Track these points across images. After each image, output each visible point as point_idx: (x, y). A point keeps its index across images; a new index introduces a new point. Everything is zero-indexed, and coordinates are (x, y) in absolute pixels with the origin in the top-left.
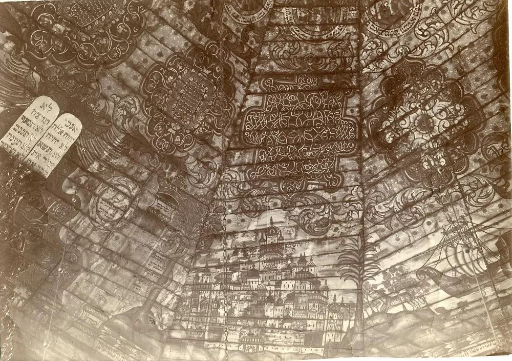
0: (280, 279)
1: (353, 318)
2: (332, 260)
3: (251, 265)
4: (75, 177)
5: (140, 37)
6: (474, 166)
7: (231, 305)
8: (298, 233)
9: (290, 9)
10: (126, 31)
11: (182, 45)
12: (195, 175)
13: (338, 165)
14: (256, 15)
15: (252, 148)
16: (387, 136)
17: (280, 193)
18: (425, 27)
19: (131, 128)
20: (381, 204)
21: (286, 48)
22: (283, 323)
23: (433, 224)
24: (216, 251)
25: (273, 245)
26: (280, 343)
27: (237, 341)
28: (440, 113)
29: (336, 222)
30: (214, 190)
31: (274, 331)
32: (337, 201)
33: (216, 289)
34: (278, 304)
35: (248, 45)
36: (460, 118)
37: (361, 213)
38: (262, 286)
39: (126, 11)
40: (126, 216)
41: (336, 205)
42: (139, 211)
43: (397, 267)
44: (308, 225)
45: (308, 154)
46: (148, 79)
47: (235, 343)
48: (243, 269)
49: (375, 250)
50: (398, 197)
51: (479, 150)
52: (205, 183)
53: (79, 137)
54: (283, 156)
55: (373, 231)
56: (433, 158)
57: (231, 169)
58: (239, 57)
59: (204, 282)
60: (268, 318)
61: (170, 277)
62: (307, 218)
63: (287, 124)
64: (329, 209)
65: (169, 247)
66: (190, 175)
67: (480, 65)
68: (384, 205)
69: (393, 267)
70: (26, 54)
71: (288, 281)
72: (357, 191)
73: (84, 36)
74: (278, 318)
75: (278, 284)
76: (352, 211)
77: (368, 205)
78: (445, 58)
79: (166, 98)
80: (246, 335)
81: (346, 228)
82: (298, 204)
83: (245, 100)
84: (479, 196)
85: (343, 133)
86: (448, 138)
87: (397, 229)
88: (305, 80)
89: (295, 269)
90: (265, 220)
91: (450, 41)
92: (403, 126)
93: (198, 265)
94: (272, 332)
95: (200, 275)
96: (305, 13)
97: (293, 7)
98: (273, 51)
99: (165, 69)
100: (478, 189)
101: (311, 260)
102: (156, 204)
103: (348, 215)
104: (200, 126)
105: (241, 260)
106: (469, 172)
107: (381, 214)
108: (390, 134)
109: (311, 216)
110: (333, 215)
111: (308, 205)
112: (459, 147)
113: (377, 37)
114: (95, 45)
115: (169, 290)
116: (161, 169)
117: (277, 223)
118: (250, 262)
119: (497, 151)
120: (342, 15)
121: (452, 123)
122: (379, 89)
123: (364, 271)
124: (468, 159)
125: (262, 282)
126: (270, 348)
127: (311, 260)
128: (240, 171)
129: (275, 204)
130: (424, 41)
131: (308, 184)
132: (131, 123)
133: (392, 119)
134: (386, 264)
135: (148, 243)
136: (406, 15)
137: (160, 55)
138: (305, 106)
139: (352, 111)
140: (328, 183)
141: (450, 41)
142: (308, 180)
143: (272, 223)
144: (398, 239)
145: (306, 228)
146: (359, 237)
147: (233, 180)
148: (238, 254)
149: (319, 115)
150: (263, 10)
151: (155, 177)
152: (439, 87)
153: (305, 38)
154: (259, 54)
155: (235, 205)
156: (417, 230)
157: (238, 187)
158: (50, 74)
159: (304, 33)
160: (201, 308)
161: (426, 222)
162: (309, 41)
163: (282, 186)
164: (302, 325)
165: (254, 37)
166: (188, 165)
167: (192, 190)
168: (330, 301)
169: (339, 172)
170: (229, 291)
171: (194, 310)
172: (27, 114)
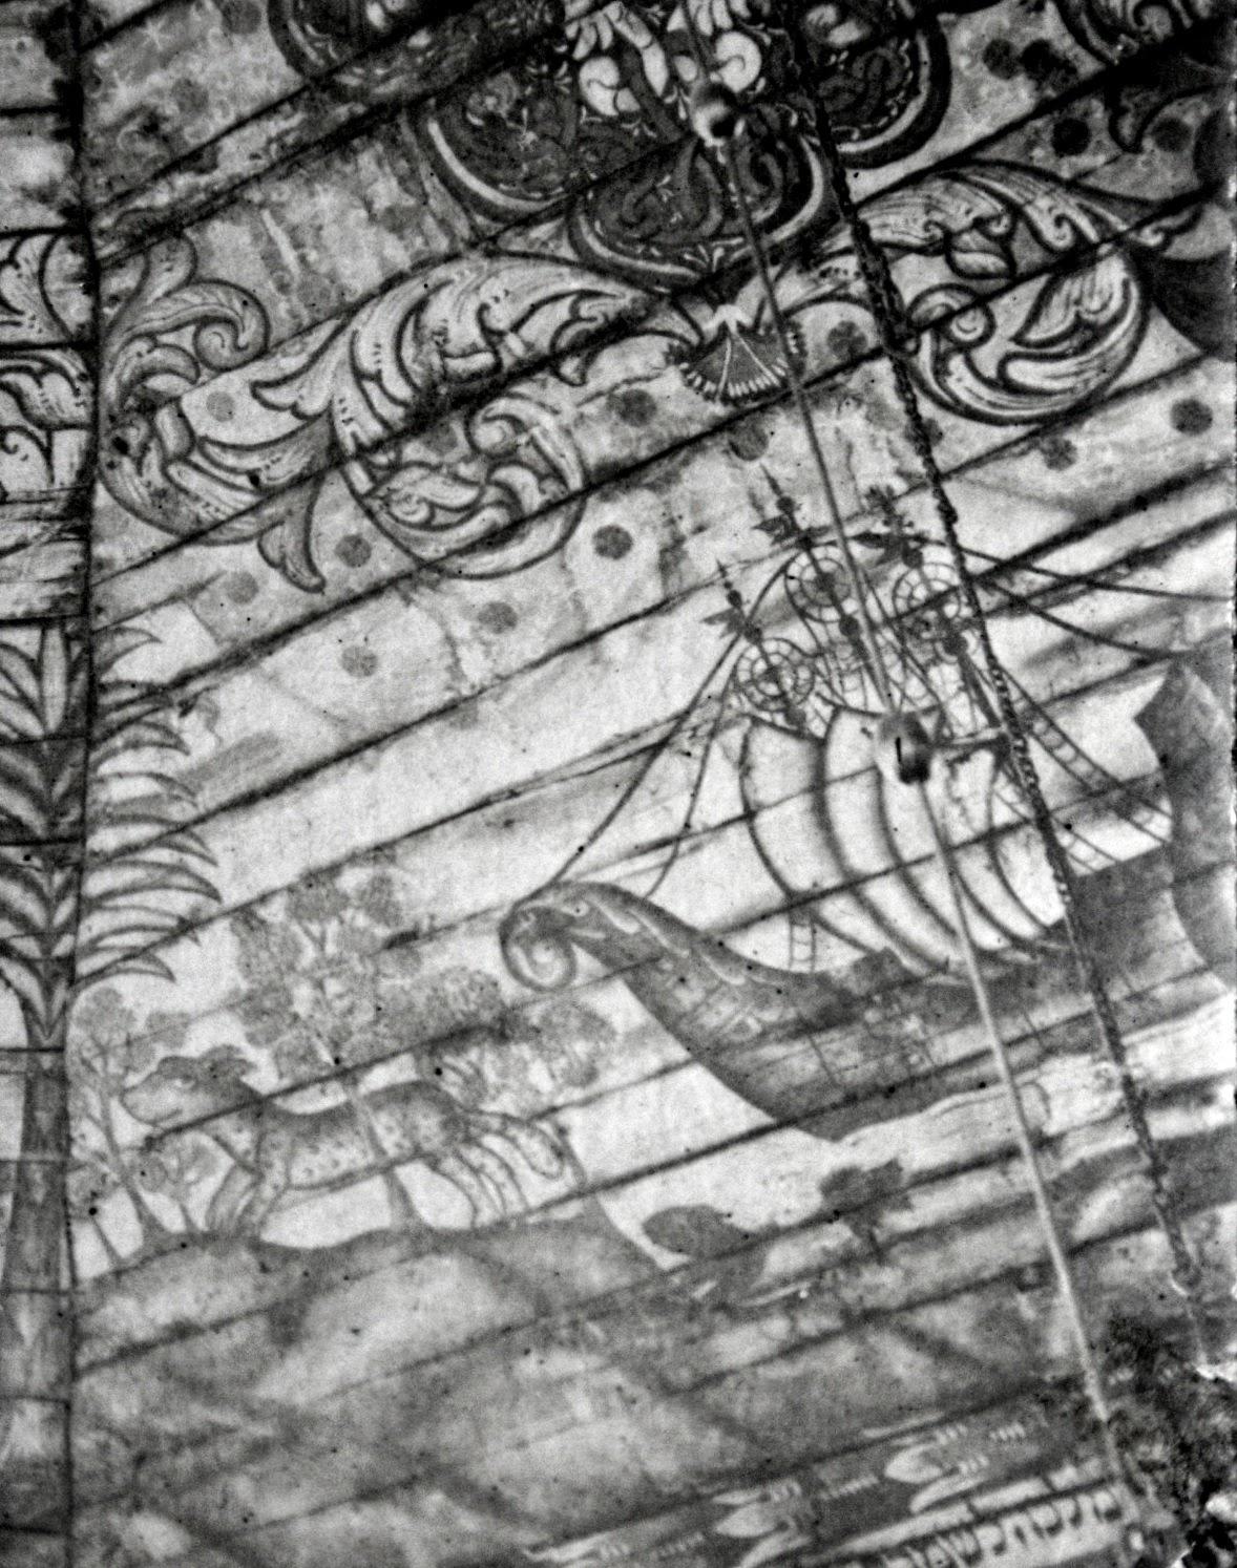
20: (234, 384)
23: (646, 548)
37: (69, 447)
43: (353, 880)
50: (375, 328)
55: (159, 595)
56: (659, 33)
68: (256, 388)
69: (320, 876)
72: (41, 275)
77: (126, 390)
84: (1018, 339)
87: (356, 581)
100: (1014, 278)
106: (948, 141)
107: (230, 460)
123: (86, 906)
144: (361, 663)
146: (55, 638)
156: (515, 591)
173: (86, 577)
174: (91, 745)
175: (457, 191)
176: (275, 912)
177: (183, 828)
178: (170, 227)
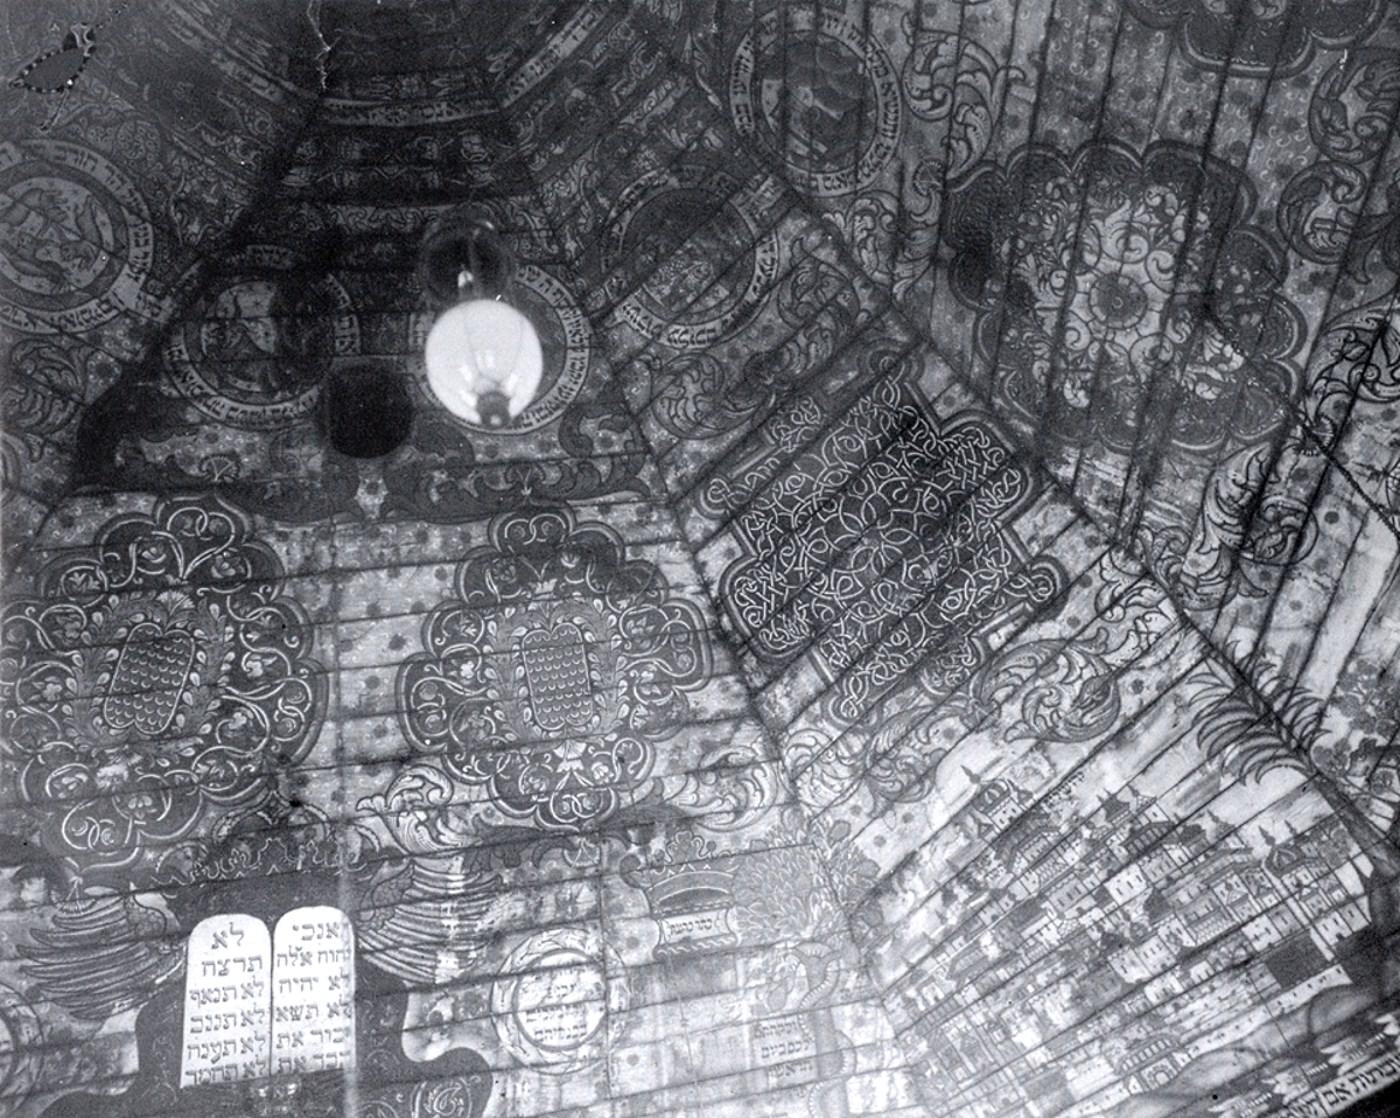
0: (1097, 883)
1: (1355, 849)
2: (1188, 755)
3: (1006, 899)
4: (421, 1018)
5: (317, 647)
6: (1313, 307)
7: (1032, 1011)
8: (1054, 758)
10: (270, 661)
11: (434, 584)
12: (715, 806)
13: (1020, 545)
15: (800, 655)
16: (1068, 394)
17: (939, 703)
18: (924, 82)
19: (465, 833)
20: (1191, 554)
22: (1187, 975)
23: (1344, 513)
24: (904, 922)
25: (1017, 823)
26: (1218, 1020)
27: (1113, 1078)
28: (1127, 247)
29: (1122, 671)
30: (794, 801)
31: (1181, 1002)
32: (1083, 623)
33: (970, 1001)
34: (1139, 941)
35: (600, 456)
36: (1180, 220)
37: (1166, 606)
38: (1069, 927)
39: (236, 624)
40: (614, 1005)
41: (1090, 632)
42: (639, 974)
43: (1352, 667)
44: (1061, 725)
45: (931, 573)
46: (411, 712)
47: (1112, 1084)
48: (994, 918)
49: (1269, 666)
50: (1211, 509)
51: (1292, 256)
52: (756, 801)
53: (357, 936)
54: (877, 618)
55: (1228, 627)
56: (1205, 364)
57: (791, 732)
58: (602, 494)
59: (933, 1003)
60: (1141, 985)
61: (843, 1043)
62: (1046, 712)
63: (830, 546)
64: (1081, 653)
65: (782, 990)
66: (701, 817)
67: (1113, 53)
68: (1197, 551)
69: (1343, 672)
70: (84, 877)
71: (1119, 876)
72: (1115, 567)
73: (182, 745)
74: (1166, 970)
75: (1102, 896)
76: (1142, 618)
77: (1167, 579)
78: (1023, 112)
79: (491, 714)
80: (1124, 1052)
81: (1158, 665)
82: (1000, 695)
83: (700, 567)
84: (1389, 365)
85: (970, 466)
86: (1195, 287)
87: (1274, 585)
88: (789, 422)
89: (1114, 838)
90: (954, 786)
91: (1001, 61)
92: (1080, 346)
93: (890, 977)
94: (1177, 1007)
95: (911, 993)
96: (667, 282)
97: (631, 292)
98: (672, 418)
99: (436, 662)
100: (1370, 349)
101: (1135, 793)
102: (667, 931)
103: (1138, 633)
104: (633, 704)
105: (972, 904)
106: (1313, 327)
107: (1210, 576)
108: (1068, 385)
109: (1053, 700)
110: (1102, 660)
111: (1024, 682)
112: (1240, 289)
113: (856, 195)
114: (226, 741)
115: (869, 1072)
116: (613, 856)
117: (986, 770)
118: (996, 896)
119: (1336, 221)
120: (746, 217)
121: (1176, 246)
122: (961, 308)
123: (1290, 728)
124: (1282, 299)
125: (1061, 916)
126: (1205, 1045)
127: (1135, 793)
128: (814, 722)
129: (949, 734)
130: (952, 116)
131: (984, 639)
132: (454, 823)
133: (1043, 350)
134: (1321, 678)
135: (718, 1018)
136: (864, 93)
137: (397, 643)
138: (835, 478)
139: (950, 402)
140: (1028, 599)
141: (1001, 61)
142: (976, 629)
143: (975, 778)
144: (1296, 606)
145: (1064, 733)
146: (1210, 661)
147: (815, 750)
148: (956, 897)
149: (882, 470)
150: (571, 354)
151: (614, 881)
152: (1072, 190)
153: (711, 335)
154: (649, 450)
155: (863, 798)
156: (1319, 552)
157: (839, 759)
158: (179, 873)
159: (701, 327)
160: (974, 1061)
161: (1321, 520)
162: (725, 333)
163: (930, 682)
164: (1237, 948)
166: (676, 802)
167: (736, 840)
168: (1261, 850)
169: (1040, 557)
170: (1003, 984)
171: (959, 1073)
172: (195, 981)
173: (1205, 637)
174: (1249, 683)
175: (1194, 453)
176: (1340, 693)
177: (1294, 687)
178: (1137, 526)
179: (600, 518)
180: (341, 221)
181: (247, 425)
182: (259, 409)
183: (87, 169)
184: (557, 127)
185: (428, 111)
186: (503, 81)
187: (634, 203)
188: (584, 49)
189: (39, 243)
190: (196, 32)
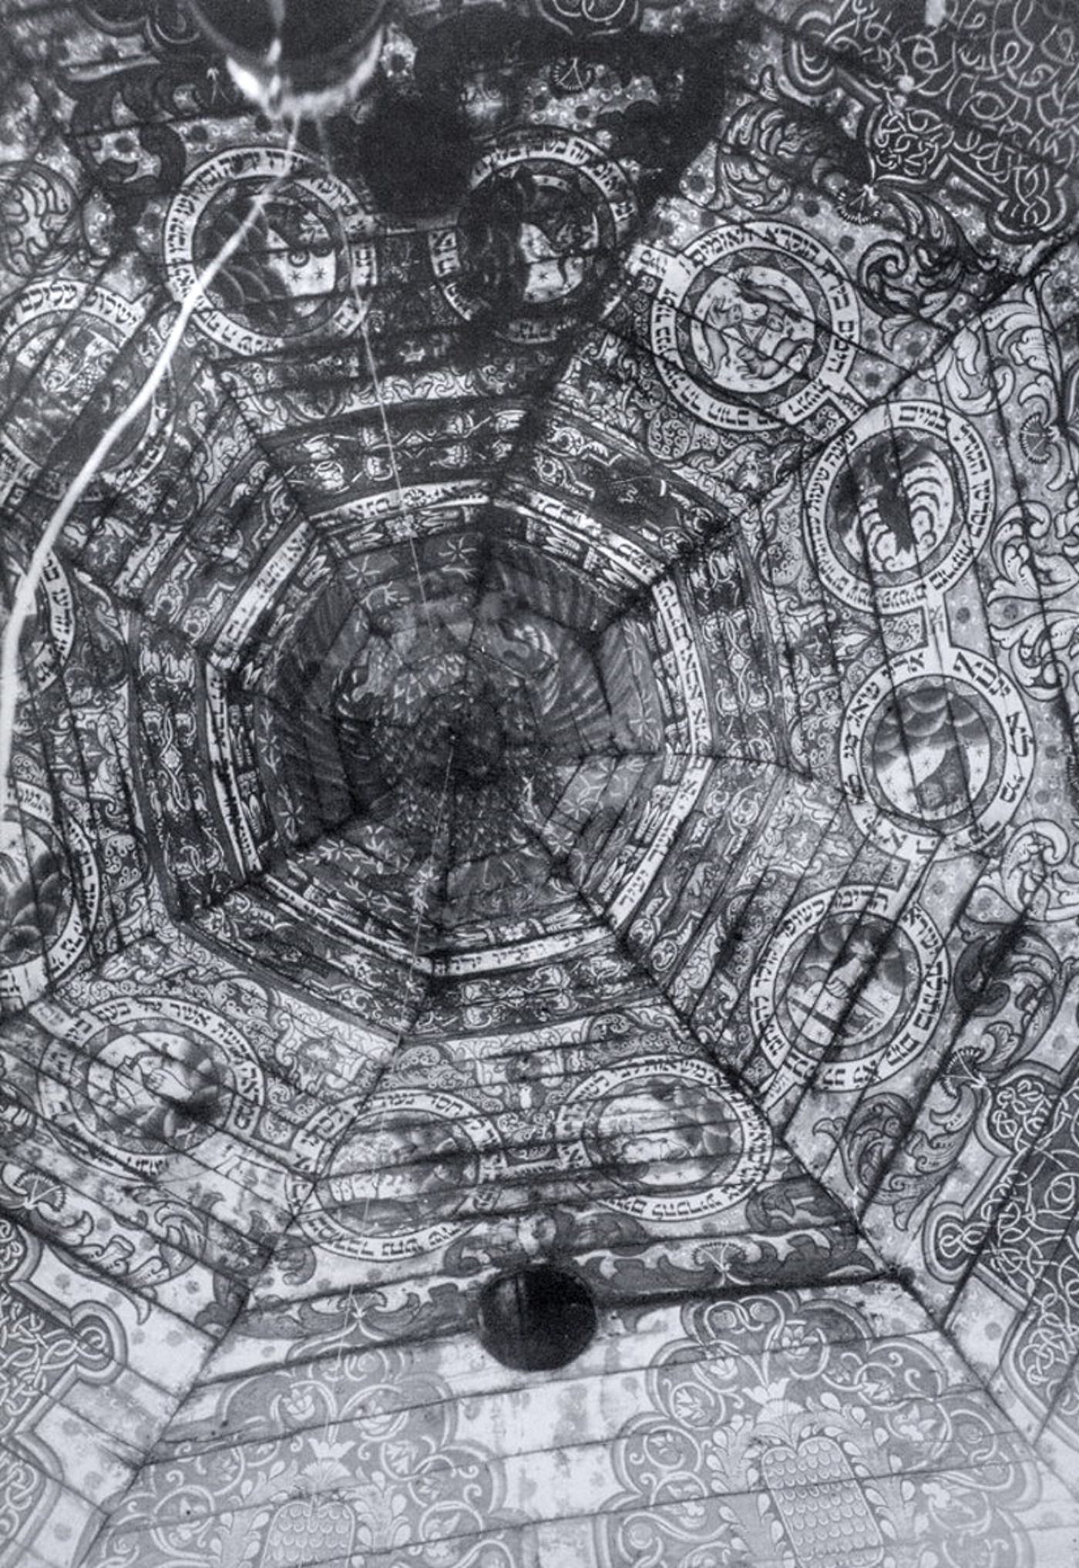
9: (129, 330)
14: (191, 222)
21: (33, 229)
35: (128, 127)
96: (93, 360)
97: (130, 342)
98: (50, 187)
120: (18, 453)
150: (187, 255)
153: (26, 303)
154: (69, 140)
159: (41, 310)
165: (135, 166)
179: (114, 41)
180: (462, 380)
181: (548, 132)
182: (534, 154)
183: (718, 404)
184: (244, 513)
185: (383, 506)
186: (308, 551)
187: (148, 447)
188: (231, 604)
189: (762, 322)
190: (618, 552)
